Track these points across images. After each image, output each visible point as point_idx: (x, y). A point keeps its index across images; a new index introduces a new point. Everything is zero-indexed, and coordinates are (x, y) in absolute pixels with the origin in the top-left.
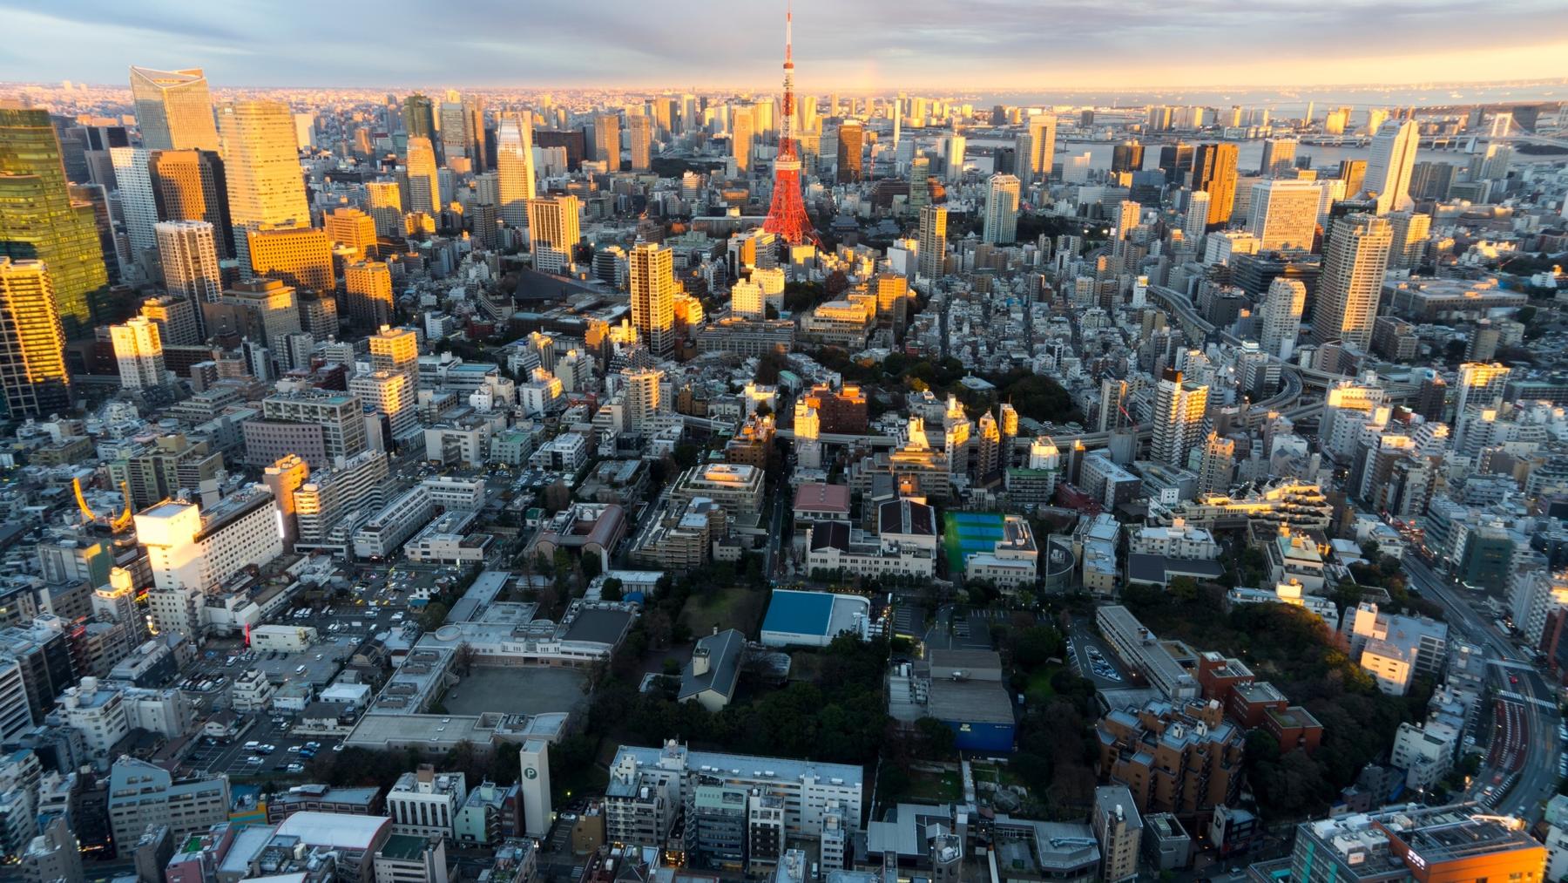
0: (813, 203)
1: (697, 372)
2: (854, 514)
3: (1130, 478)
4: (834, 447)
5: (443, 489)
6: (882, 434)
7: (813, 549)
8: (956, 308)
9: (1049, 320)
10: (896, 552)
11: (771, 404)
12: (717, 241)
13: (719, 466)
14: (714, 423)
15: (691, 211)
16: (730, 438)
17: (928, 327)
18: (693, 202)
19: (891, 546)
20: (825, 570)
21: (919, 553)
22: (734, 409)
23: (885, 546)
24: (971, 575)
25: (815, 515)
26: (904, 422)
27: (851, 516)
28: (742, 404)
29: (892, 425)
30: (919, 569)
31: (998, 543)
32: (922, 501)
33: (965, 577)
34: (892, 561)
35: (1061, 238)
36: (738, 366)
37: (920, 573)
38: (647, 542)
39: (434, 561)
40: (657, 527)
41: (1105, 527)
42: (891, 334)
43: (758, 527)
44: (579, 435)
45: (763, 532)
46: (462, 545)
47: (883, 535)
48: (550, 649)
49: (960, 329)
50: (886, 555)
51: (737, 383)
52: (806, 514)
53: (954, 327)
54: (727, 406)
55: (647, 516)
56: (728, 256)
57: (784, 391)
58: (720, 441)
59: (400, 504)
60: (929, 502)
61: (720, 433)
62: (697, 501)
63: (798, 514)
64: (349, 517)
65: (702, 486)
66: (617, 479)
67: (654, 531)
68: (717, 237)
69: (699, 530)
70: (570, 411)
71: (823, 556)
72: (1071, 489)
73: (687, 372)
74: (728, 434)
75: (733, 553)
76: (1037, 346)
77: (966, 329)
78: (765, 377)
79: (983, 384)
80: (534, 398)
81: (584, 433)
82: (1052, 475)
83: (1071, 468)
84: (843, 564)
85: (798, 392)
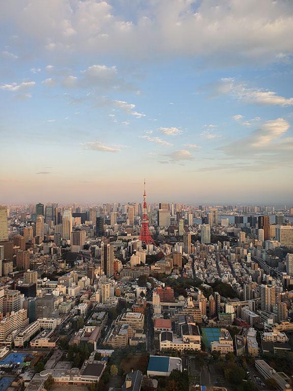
3: (257, 316)
5: (43, 322)
7: (161, 341)
10: (188, 341)
14: (127, 300)
16: (133, 304)
24: (213, 349)
27: (172, 330)
31: (220, 338)
32: (194, 324)
34: (187, 345)
37: (196, 349)
39: (39, 347)
40: (111, 334)
41: (252, 332)
42: (178, 272)
46: (49, 341)
47: (184, 336)
48: (77, 379)
52: (158, 329)
55: (108, 330)
57: (148, 289)
58: (130, 305)
59: (30, 327)
60: (196, 324)
63: (156, 329)
64: (14, 332)
65: (125, 320)
66: (98, 318)
71: (165, 344)
72: (239, 320)
75: (136, 343)
78: (141, 284)
79: (209, 286)
80: (73, 292)
81: (87, 303)
82: (233, 315)
83: (238, 313)
85: (152, 289)
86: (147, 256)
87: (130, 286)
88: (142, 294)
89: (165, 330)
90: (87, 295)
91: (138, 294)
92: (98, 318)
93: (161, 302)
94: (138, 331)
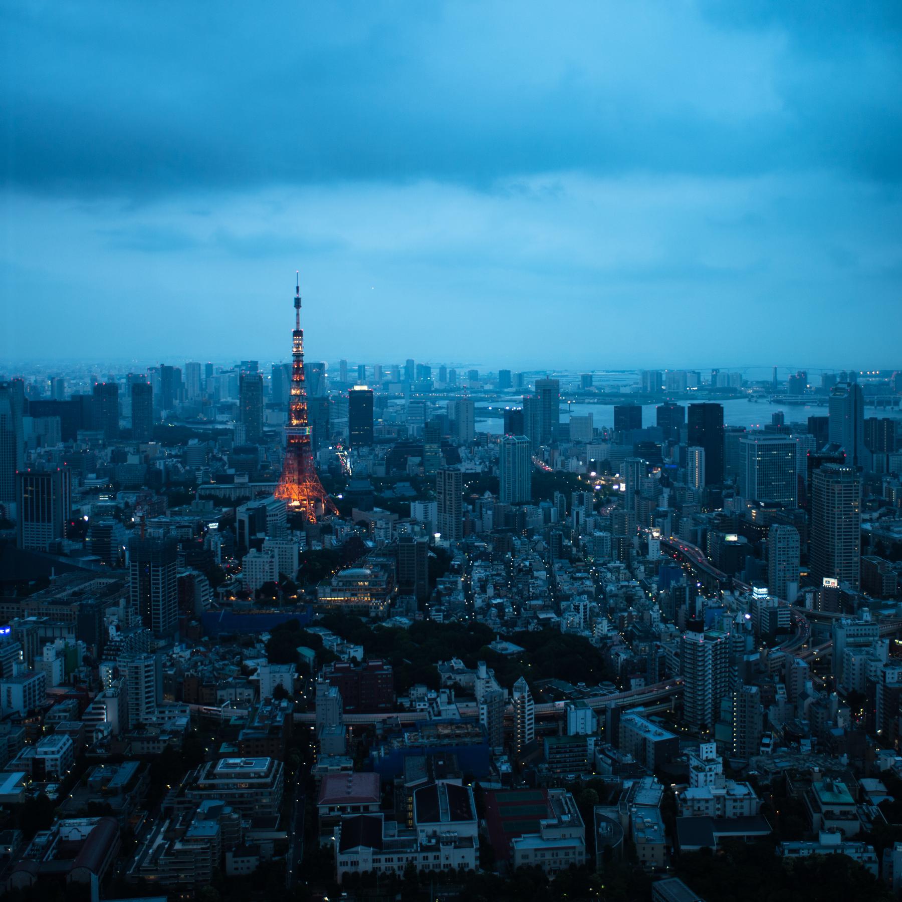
0: (325, 467)
1: (204, 655)
2: (385, 805)
4: (360, 729)
6: (412, 709)
8: (478, 573)
9: (572, 578)
11: (288, 686)
12: (224, 510)
13: (231, 761)
15: (196, 478)
16: (243, 727)
17: (450, 591)
18: (199, 470)
19: (429, 838)
20: (356, 873)
21: (462, 842)
22: (248, 693)
23: (422, 838)
25: (343, 809)
26: (433, 695)
27: (382, 808)
28: (256, 686)
29: (421, 699)
30: (461, 861)
31: (544, 822)
32: (458, 783)
33: (512, 865)
34: (431, 855)
35: (575, 495)
36: (250, 644)
37: (462, 866)
38: (147, 860)
40: (159, 840)
43: (280, 830)
44: (66, 736)
45: (284, 835)
47: (420, 827)
49: (483, 589)
50: (425, 849)
51: (250, 663)
53: (478, 589)
54: (239, 691)
55: (147, 828)
56: (237, 525)
61: (232, 722)
62: (206, 805)
63: (323, 810)
65: (212, 787)
67: (155, 846)
68: (225, 506)
69: (210, 840)
70: (56, 707)
71: (354, 858)
73: (192, 654)
74: (240, 722)
76: (564, 604)
77: (490, 591)
81: (72, 733)
84: (376, 865)
86: (302, 557)
87: (239, 663)
88: (279, 693)
89: (355, 809)
90: (70, 703)
91: (266, 690)
92: (111, 785)
93: (346, 712)
94: (262, 823)
